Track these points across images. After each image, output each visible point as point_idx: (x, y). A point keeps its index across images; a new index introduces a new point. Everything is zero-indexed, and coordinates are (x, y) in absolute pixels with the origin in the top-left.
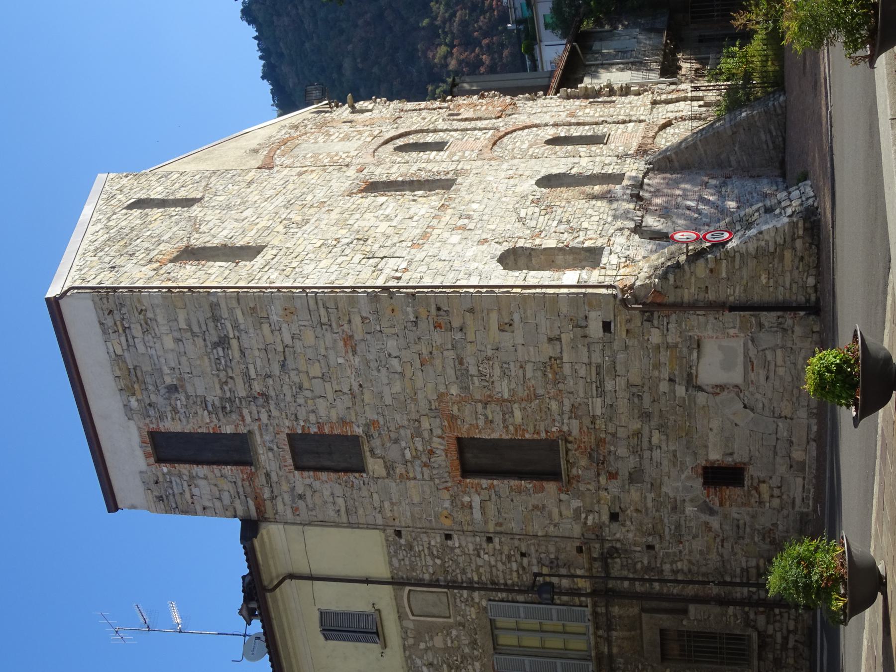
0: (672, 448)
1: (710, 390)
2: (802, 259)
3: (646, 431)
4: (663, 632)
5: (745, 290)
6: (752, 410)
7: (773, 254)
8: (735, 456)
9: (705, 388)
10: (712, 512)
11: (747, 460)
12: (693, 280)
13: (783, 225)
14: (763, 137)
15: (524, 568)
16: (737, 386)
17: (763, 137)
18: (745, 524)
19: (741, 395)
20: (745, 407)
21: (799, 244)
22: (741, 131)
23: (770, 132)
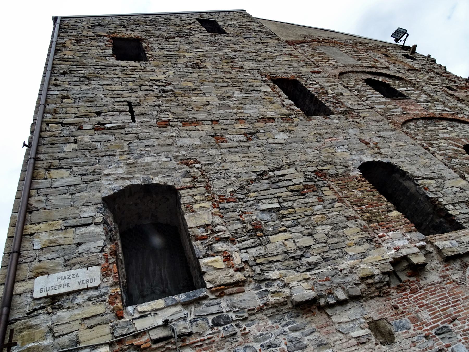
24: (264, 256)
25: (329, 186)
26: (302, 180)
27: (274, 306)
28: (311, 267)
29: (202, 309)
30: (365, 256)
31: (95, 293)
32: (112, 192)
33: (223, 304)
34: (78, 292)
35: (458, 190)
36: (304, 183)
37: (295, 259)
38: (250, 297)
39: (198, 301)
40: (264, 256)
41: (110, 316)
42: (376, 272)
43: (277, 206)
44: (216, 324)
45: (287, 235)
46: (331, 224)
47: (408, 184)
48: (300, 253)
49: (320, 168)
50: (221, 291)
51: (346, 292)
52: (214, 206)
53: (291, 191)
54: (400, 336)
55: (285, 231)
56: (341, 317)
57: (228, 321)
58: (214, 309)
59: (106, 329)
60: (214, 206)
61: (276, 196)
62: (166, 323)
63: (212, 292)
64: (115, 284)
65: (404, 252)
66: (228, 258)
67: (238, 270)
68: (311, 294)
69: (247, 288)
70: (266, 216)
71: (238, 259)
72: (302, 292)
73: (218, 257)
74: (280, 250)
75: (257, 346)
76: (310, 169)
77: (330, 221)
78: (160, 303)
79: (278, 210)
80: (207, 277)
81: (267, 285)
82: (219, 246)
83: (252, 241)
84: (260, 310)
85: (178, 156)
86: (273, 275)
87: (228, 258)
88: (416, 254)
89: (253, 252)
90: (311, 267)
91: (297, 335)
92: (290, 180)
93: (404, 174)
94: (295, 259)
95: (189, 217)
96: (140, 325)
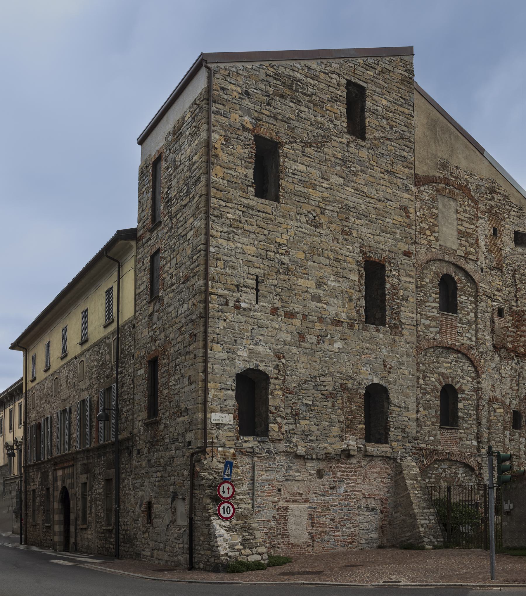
0: (157, 484)
1: (173, 505)
2: (208, 561)
3: (161, 469)
4: (111, 479)
5: (199, 527)
6: (167, 530)
7: (209, 545)
8: (155, 520)
9: (174, 502)
10: (141, 506)
11: (154, 526)
12: (202, 496)
13: (218, 551)
14: (408, 534)
15: (126, 402)
16: (175, 521)
17: (408, 534)
18: (138, 524)
19: (171, 524)
20: (168, 526)
21: (212, 559)
22: (412, 520)
23: (409, 539)
24: (294, 430)
25: (342, 397)
26: (331, 388)
27: (289, 452)
28: (310, 441)
29: (264, 446)
30: (333, 444)
31: (231, 427)
32: (240, 371)
33: (272, 446)
34: (225, 424)
35: (406, 419)
36: (331, 391)
37: (305, 435)
38: (282, 446)
39: (264, 442)
40: (294, 430)
41: (235, 438)
42: (333, 453)
43: (311, 403)
44: (267, 452)
45: (308, 422)
46: (330, 422)
47: (386, 404)
48: (309, 433)
49: (345, 381)
50: (273, 441)
51: (317, 456)
52: (283, 395)
53: (322, 394)
54: (325, 478)
55: (308, 420)
56: (309, 464)
57: (271, 452)
58: (268, 447)
59: (233, 443)
60: (283, 395)
61: (313, 396)
62: (252, 448)
63: (270, 440)
64: (237, 425)
65: (350, 448)
66: (280, 427)
67: (282, 434)
68: (304, 453)
69: (282, 442)
70: (303, 408)
71: (284, 428)
72: (301, 451)
73: (276, 425)
74: (301, 429)
75: (277, 464)
76: (340, 381)
77: (330, 420)
78: (251, 438)
79: (310, 405)
80: (270, 434)
81: (290, 443)
82: (279, 420)
83: (292, 420)
84: (283, 452)
85: (276, 349)
86: (294, 440)
87: (280, 427)
88: (354, 450)
89: (291, 426)
90: (310, 441)
91: (291, 465)
92: (325, 386)
93: (388, 398)
94: (305, 435)
95: (271, 398)
96: (245, 445)
